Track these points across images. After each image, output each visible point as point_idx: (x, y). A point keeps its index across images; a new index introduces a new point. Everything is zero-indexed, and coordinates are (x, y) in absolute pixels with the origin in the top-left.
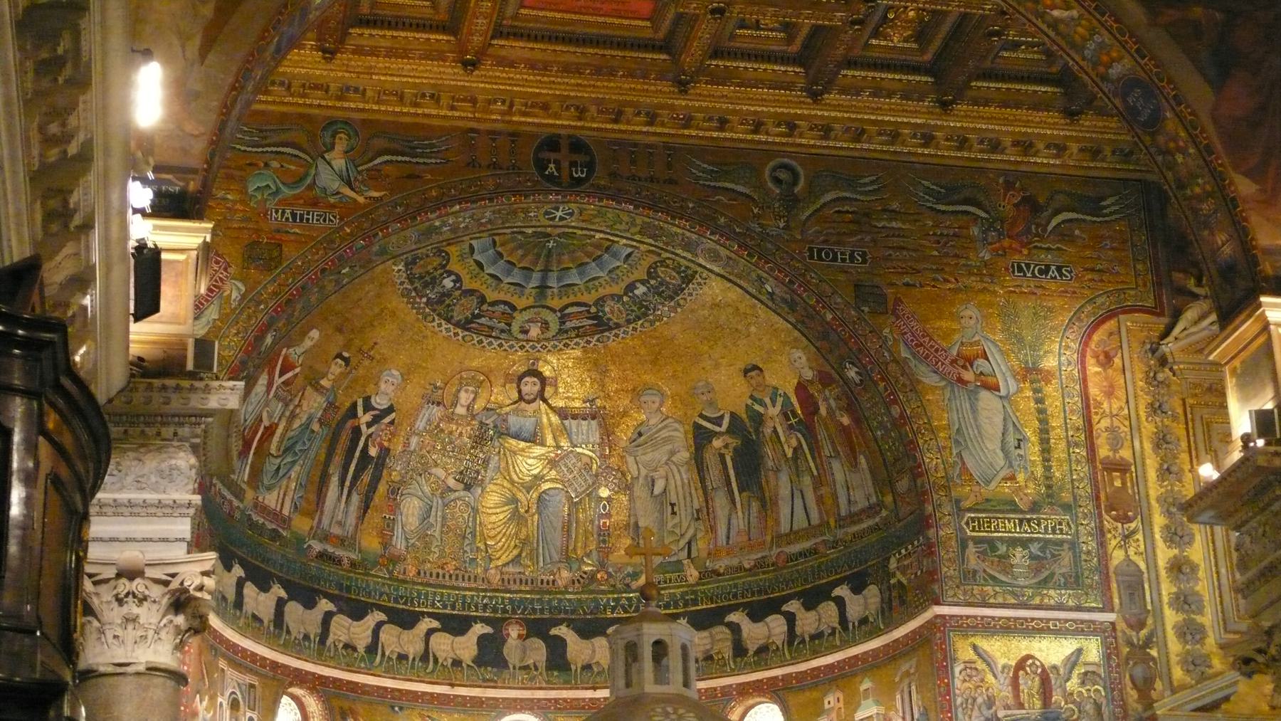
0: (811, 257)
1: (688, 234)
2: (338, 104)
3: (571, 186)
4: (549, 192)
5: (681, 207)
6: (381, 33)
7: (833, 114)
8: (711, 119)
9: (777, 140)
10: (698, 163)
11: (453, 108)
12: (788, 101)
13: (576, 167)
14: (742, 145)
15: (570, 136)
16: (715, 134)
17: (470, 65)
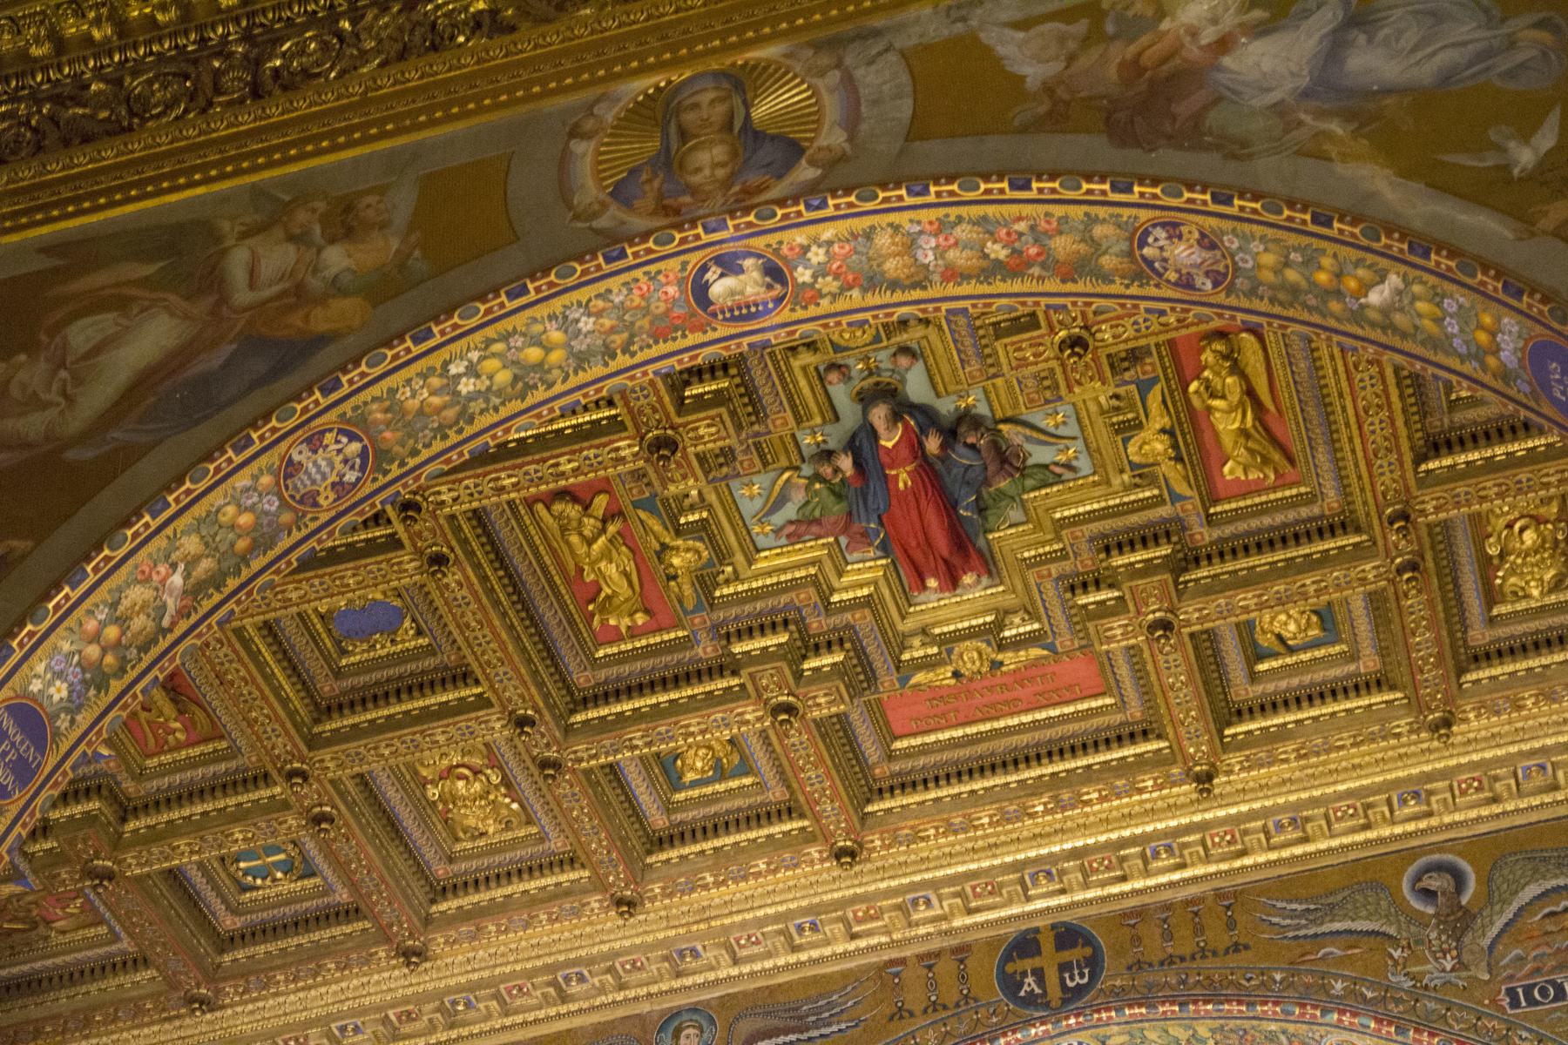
0: (1515, 1003)
1: (1291, 1028)
2: (676, 984)
3: (1065, 1002)
4: (1029, 1023)
5: (1263, 983)
6: (697, 848)
7: (1488, 755)
8: (1280, 827)
9: (1411, 827)
10: (1279, 905)
11: (854, 937)
12: (1400, 756)
13: (1071, 970)
14: (1352, 856)
15: (1054, 927)
16: (1298, 850)
17: (846, 855)
